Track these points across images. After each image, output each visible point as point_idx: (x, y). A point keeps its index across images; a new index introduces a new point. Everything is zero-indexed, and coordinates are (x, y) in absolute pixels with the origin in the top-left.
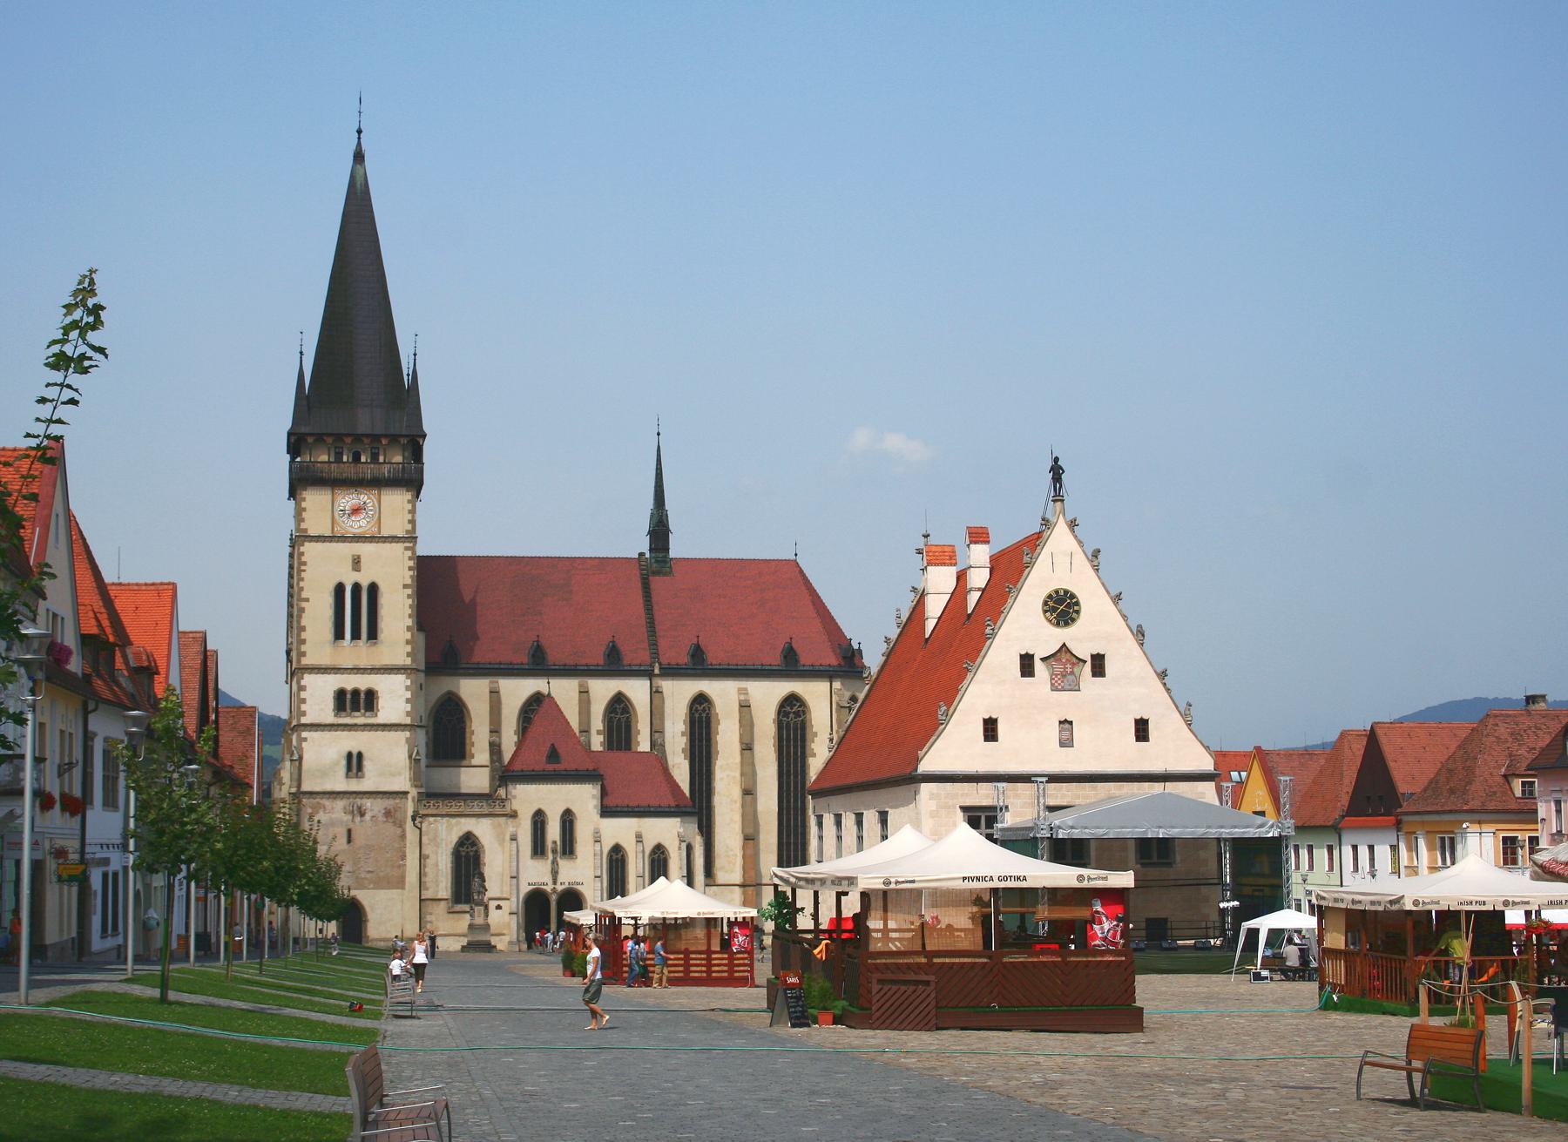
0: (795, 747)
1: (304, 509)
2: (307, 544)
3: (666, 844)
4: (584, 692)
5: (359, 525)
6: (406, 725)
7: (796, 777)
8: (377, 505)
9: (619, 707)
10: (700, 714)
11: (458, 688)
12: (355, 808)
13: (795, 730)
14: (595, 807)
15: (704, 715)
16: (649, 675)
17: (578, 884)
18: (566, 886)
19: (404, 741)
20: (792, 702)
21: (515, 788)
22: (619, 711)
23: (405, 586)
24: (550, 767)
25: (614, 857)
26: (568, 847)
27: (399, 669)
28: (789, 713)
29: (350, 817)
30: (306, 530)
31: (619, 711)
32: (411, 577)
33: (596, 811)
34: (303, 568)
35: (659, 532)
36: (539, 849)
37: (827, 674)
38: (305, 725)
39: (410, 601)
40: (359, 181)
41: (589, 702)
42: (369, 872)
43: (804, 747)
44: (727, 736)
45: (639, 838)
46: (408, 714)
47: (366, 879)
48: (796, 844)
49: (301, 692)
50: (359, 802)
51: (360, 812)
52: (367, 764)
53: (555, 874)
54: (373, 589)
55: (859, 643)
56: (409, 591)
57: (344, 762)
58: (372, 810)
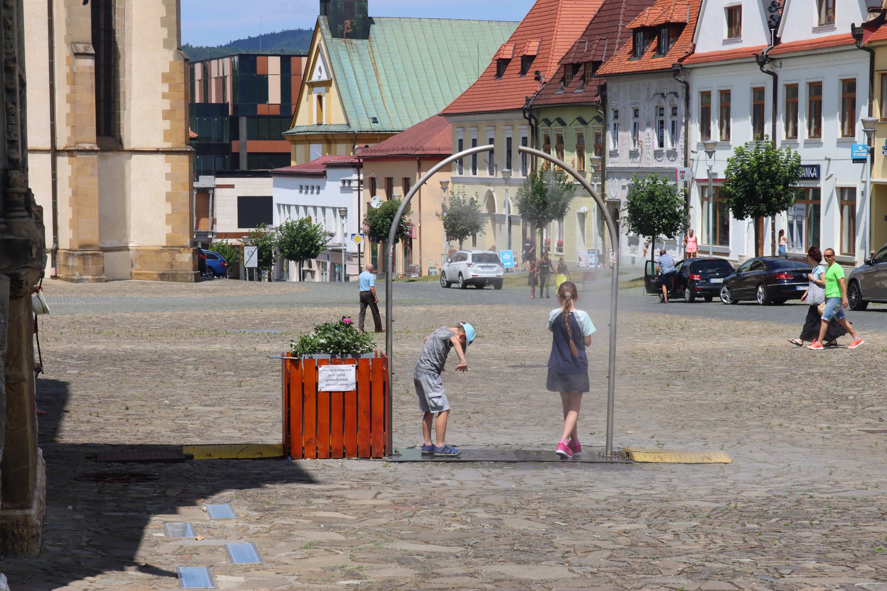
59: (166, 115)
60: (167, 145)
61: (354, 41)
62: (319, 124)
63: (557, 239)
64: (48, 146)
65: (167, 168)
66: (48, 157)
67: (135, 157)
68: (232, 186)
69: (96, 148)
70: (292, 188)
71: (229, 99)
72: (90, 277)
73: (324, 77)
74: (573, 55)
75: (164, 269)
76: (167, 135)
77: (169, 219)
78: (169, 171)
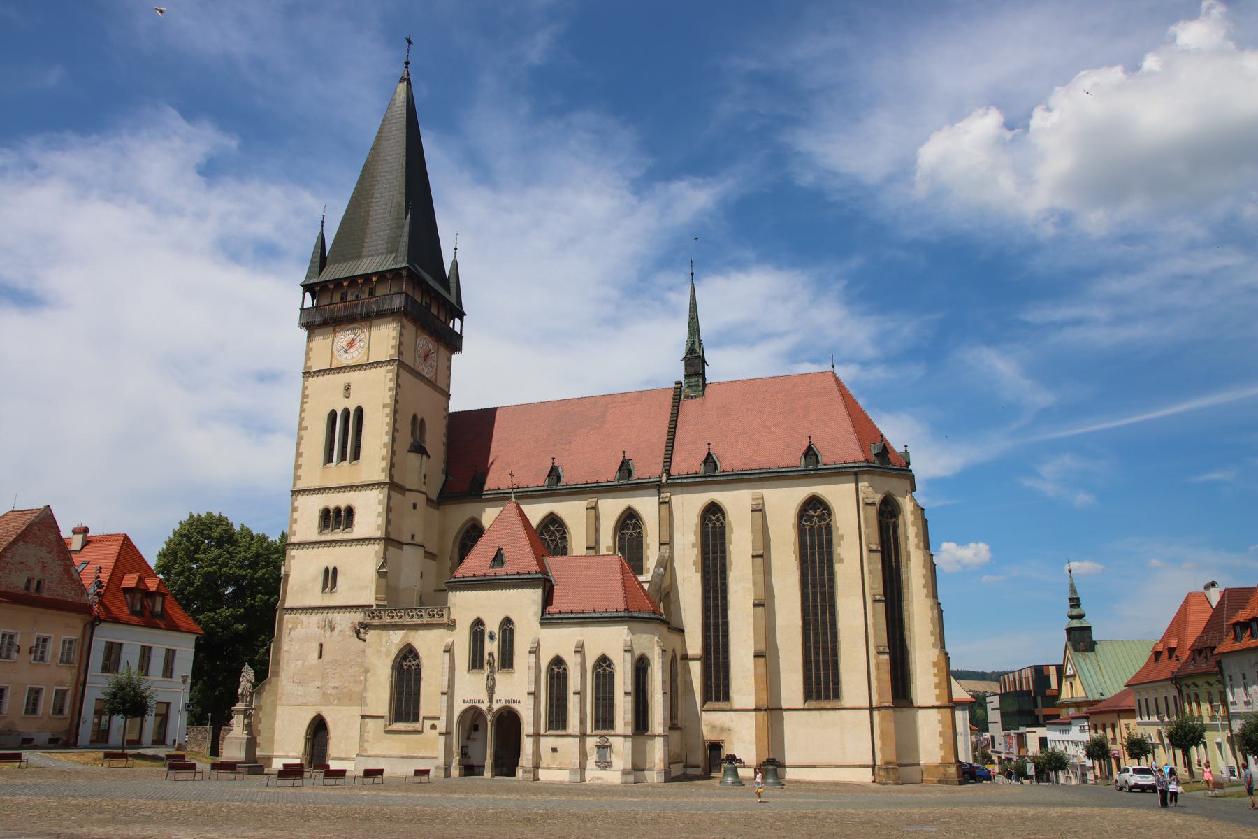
0: (821, 554)
1: (311, 349)
2: (310, 379)
3: (611, 656)
4: (595, 508)
5: (355, 356)
6: (375, 539)
7: (823, 586)
8: (368, 337)
9: (630, 519)
10: (714, 524)
11: (481, 516)
12: (327, 623)
13: (820, 535)
14: (535, 613)
15: (718, 525)
16: (658, 487)
17: (515, 702)
18: (502, 704)
19: (373, 552)
20: (815, 504)
21: (455, 596)
22: (631, 527)
23: (385, 406)
24: (491, 572)
25: (556, 670)
26: (507, 660)
27: (373, 485)
28: (813, 516)
29: (323, 632)
30: (311, 367)
31: (631, 527)
32: (390, 397)
33: (535, 618)
34: (305, 400)
35: (695, 361)
36: (476, 662)
37: (852, 473)
38: (294, 544)
39: (388, 420)
40: (410, 96)
41: (597, 518)
42: (334, 687)
43: (830, 554)
44: (740, 544)
45: (580, 650)
46: (379, 527)
47: (331, 694)
48: (826, 662)
49: (294, 513)
50: (330, 615)
51: (331, 626)
52: (338, 578)
53: (491, 690)
54: (360, 412)
55: (906, 446)
56: (388, 410)
57: (321, 578)
58: (341, 625)
59: (937, 686)
60: (938, 703)
61: (1087, 654)
62: (1072, 697)
63: (1197, 758)
64: (868, 705)
65: (939, 717)
66: (868, 711)
67: (920, 710)
68: (1035, 732)
69: (892, 705)
70: (1055, 731)
71: (1031, 688)
72: (891, 782)
73: (1072, 673)
74: (1196, 644)
75: (940, 777)
76: (938, 698)
77: (942, 747)
78: (940, 718)
